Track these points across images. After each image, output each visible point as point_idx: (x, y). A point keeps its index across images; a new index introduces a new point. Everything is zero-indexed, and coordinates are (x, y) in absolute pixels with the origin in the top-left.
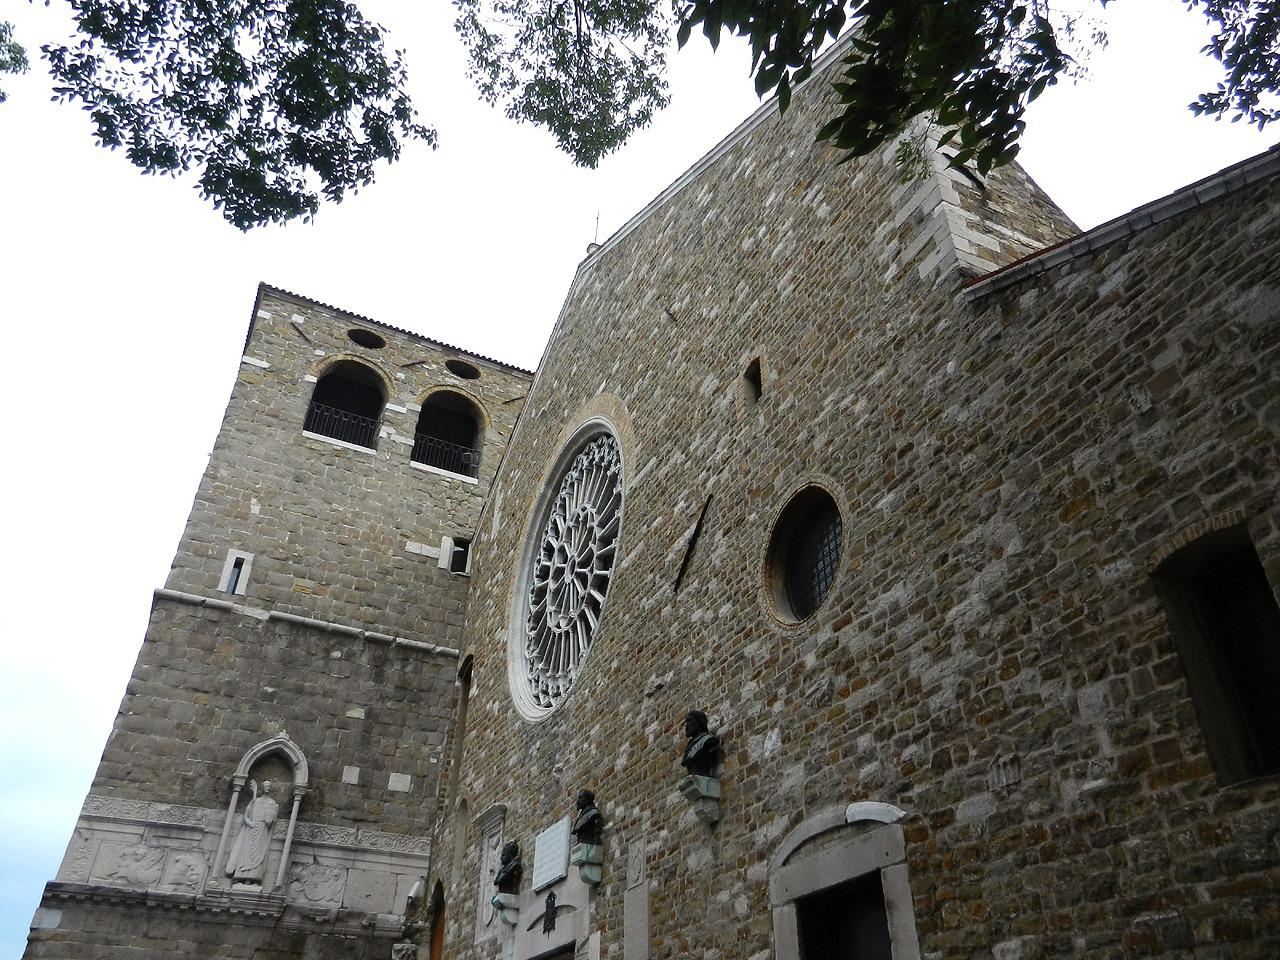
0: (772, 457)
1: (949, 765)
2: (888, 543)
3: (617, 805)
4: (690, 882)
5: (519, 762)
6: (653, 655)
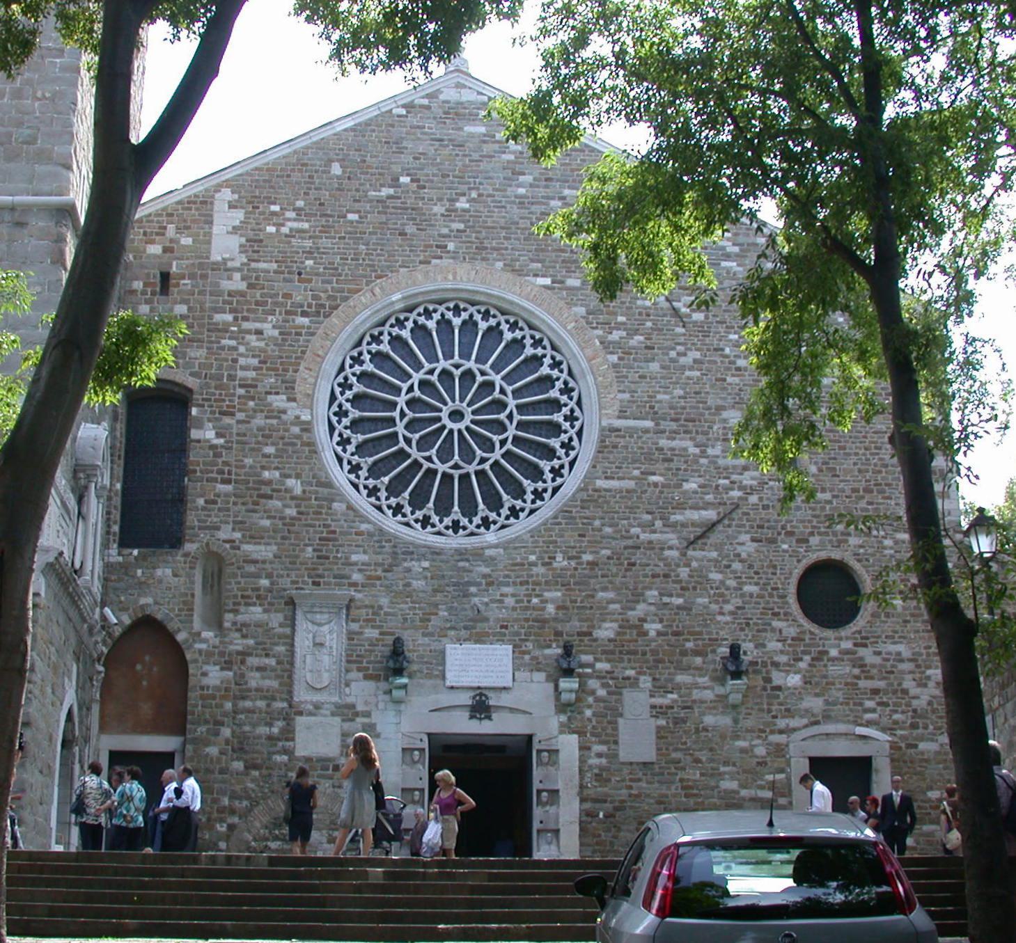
0: (810, 521)
1: (918, 728)
2: (898, 623)
3: (596, 660)
4: (707, 731)
6: (654, 576)
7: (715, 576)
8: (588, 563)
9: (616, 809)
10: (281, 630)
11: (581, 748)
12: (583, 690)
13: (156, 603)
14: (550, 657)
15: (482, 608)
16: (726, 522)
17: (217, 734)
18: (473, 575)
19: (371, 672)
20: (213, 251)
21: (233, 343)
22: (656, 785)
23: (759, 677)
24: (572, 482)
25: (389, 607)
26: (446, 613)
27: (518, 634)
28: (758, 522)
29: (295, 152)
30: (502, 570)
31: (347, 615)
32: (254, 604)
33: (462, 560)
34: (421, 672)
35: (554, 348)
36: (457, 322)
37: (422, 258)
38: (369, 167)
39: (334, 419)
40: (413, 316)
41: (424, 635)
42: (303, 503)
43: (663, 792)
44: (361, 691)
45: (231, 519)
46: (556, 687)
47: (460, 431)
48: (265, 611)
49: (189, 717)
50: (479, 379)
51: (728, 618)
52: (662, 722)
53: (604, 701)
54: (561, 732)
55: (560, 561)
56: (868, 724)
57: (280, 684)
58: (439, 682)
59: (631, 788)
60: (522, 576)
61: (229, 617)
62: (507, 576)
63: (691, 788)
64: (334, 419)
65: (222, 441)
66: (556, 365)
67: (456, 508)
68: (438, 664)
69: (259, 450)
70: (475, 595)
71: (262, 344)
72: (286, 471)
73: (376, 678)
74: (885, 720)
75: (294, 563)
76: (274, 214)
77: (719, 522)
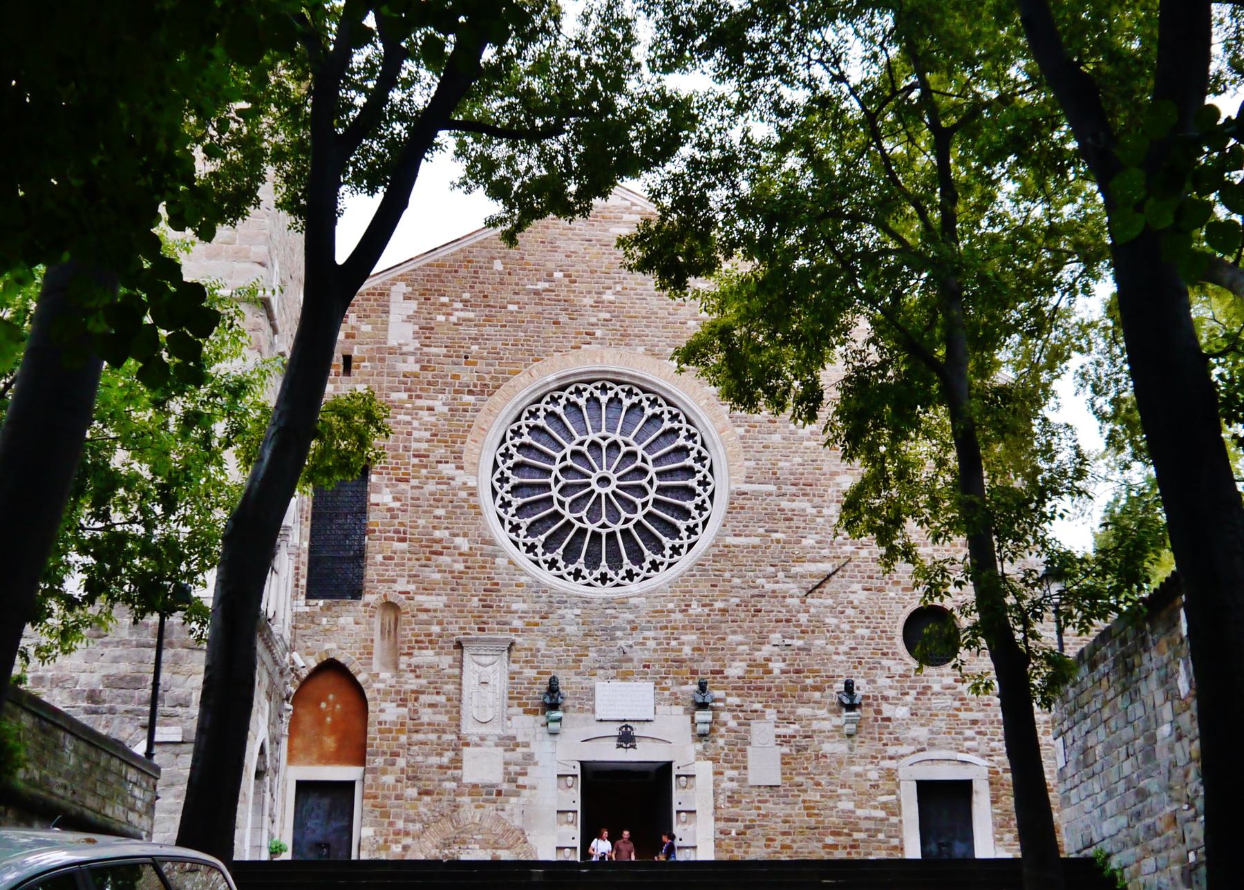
5: (538, 612)
6: (777, 621)
7: (831, 621)
8: (720, 610)
9: (747, 827)
10: (450, 671)
11: (716, 773)
12: (715, 721)
13: (340, 648)
15: (627, 649)
16: (840, 573)
17: (393, 764)
18: (619, 621)
20: (389, 337)
21: (408, 418)
22: (782, 806)
23: (871, 709)
24: (705, 539)
27: (658, 673)
28: (868, 573)
29: (462, 250)
32: (427, 648)
35: (689, 422)
36: (604, 399)
37: (573, 344)
38: (527, 264)
39: (497, 485)
40: (565, 394)
41: (577, 674)
42: (470, 559)
43: (789, 812)
44: (525, 725)
45: (406, 573)
46: (693, 719)
47: (607, 495)
48: (438, 654)
49: (368, 749)
50: (624, 449)
51: (843, 658)
52: (786, 750)
54: (697, 759)
55: (695, 609)
56: (969, 751)
57: (450, 719)
58: (589, 715)
59: (759, 808)
61: (404, 660)
63: (813, 808)
64: (497, 485)
65: (397, 505)
66: (691, 436)
67: (604, 562)
68: (589, 700)
69: (431, 512)
71: (433, 419)
72: (456, 531)
73: (535, 712)
74: (984, 749)
75: (462, 611)
76: (443, 305)
77: (834, 573)
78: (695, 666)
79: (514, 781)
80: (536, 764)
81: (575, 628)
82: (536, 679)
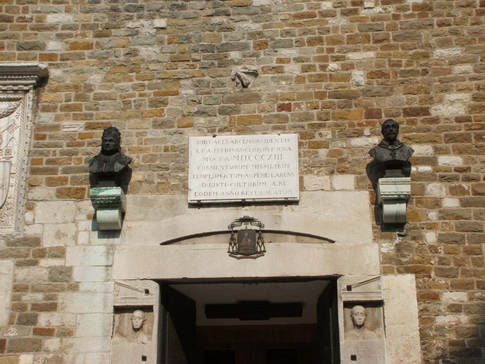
3: (438, 151)
14: (361, 149)
19: (69, 186)
25: (101, 87)
26: (191, 92)
27: (307, 117)
30: (279, 26)
31: (37, 102)
33: (217, 14)
34: (151, 182)
53: (458, 218)
54: (385, 272)
58: (178, 196)
60: (310, 31)
62: (288, 33)
70: (237, 64)
73: (78, 195)
78: (375, 103)
79: (31, 320)
80: (74, 288)
81: (157, 49)
82: (82, 136)
